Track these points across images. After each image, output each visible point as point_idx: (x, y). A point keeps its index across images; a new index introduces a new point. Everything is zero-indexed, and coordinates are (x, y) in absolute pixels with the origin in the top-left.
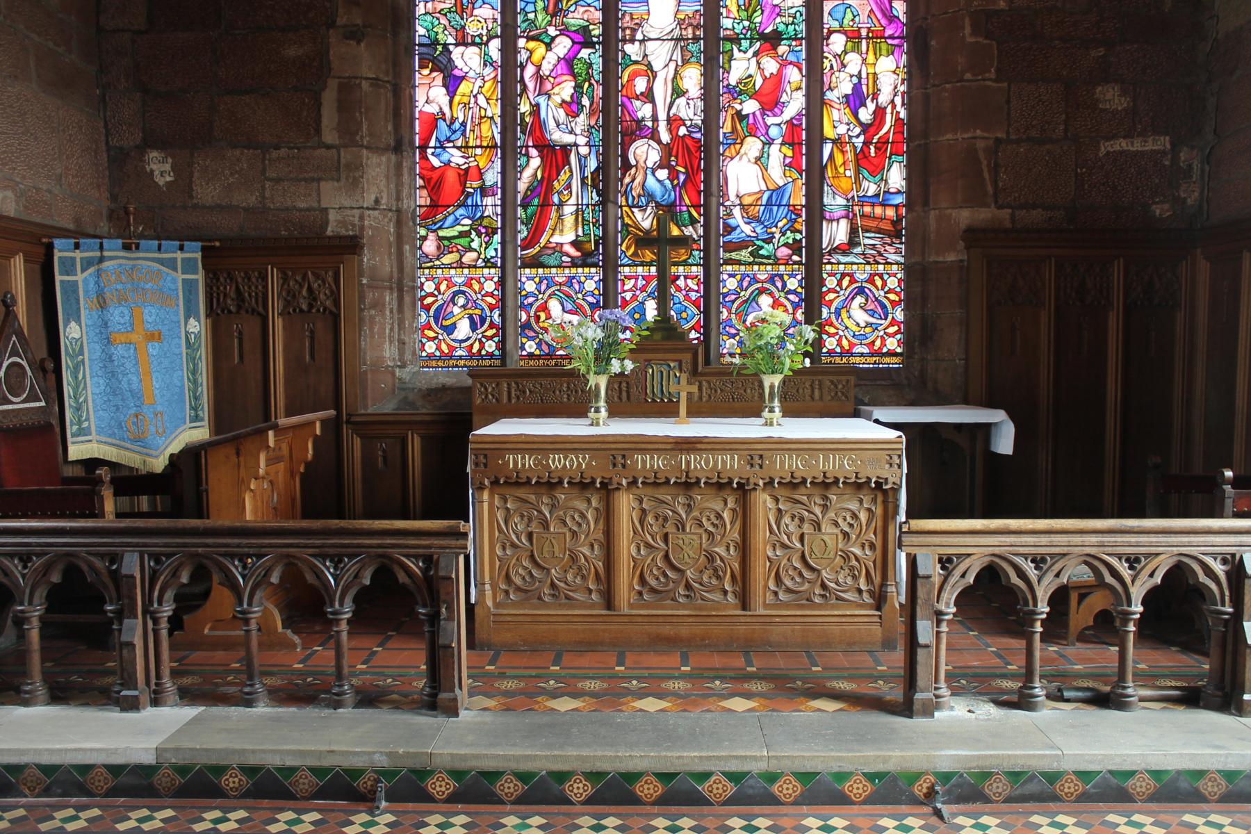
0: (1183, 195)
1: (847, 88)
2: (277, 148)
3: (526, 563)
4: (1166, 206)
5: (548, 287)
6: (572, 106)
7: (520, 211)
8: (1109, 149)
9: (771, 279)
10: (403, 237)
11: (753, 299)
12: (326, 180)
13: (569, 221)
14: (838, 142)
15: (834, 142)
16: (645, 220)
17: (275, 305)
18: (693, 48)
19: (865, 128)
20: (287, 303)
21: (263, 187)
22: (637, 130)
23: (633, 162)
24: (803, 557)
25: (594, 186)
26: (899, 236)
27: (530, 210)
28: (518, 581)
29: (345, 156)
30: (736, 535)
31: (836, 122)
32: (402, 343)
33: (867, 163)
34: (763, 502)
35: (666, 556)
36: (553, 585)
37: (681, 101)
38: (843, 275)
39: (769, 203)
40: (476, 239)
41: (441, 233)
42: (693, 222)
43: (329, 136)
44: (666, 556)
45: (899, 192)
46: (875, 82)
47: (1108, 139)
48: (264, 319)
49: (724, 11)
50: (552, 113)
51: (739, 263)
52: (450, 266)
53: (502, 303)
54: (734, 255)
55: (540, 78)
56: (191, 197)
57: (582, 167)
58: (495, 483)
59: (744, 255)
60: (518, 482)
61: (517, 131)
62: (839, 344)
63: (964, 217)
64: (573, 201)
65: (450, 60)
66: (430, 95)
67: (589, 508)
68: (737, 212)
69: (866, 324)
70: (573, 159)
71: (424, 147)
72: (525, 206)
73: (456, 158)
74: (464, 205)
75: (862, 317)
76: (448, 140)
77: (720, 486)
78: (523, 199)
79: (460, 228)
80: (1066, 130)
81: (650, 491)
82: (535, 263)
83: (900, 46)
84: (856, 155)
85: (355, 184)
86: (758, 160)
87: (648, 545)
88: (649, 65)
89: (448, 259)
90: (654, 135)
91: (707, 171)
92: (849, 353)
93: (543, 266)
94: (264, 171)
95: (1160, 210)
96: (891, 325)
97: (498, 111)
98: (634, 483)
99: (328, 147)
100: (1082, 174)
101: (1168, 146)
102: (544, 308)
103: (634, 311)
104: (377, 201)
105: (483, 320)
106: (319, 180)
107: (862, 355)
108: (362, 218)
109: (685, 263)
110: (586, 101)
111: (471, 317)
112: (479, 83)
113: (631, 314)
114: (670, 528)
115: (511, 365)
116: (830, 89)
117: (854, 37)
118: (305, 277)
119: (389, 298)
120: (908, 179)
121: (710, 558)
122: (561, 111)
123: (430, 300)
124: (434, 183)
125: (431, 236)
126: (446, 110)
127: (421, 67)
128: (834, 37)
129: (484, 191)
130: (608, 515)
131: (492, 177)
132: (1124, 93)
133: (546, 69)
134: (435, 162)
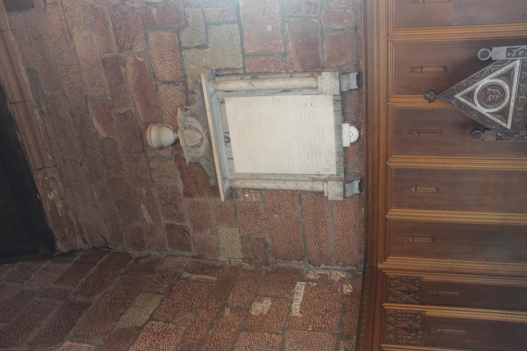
0: (339, 278)
4: (345, 286)
8: (297, 311)
47: (290, 310)
80: (278, 334)
95: (347, 289)
100: (313, 327)
101: (304, 283)
132: (260, 301)
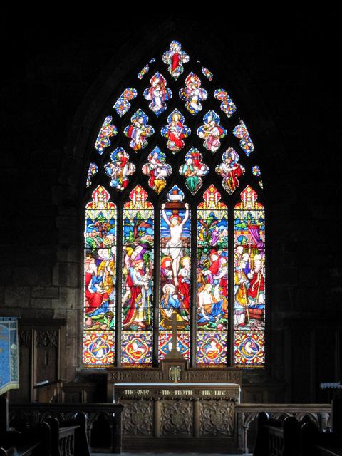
1: (244, 266)
2: (36, 286)
3: (130, 423)
5: (133, 338)
6: (143, 272)
7: (122, 310)
9: (215, 336)
10: (79, 319)
11: (209, 343)
12: (54, 298)
13: (141, 313)
14: (241, 286)
15: (239, 285)
16: (169, 313)
17: (34, 343)
18: (186, 250)
19: (250, 281)
20: (39, 343)
21: (31, 301)
22: (166, 280)
23: (165, 292)
24: (211, 421)
25: (151, 300)
26: (262, 320)
27: (127, 309)
28: (127, 428)
29: (61, 290)
30: (191, 415)
31: (239, 278)
32: (79, 358)
33: (251, 293)
34: (199, 404)
35: (171, 421)
36: (137, 429)
37: (182, 270)
38: (243, 334)
39: (214, 309)
40: (106, 320)
41: (93, 318)
42: (187, 314)
43: (56, 283)
44: (171, 421)
45: (263, 304)
46: (254, 265)
48: (30, 349)
49: (198, 238)
50: (136, 275)
51: (203, 330)
52: (96, 330)
53: (116, 342)
54: (202, 327)
55: (131, 261)
56: (4, 303)
57: (146, 294)
58: (121, 398)
59: (206, 327)
60: (129, 398)
61: (120, 281)
62: (241, 360)
63: (283, 315)
64: (142, 306)
65: (97, 254)
66: (90, 267)
67: (149, 407)
68: (203, 311)
69: (251, 351)
70: (143, 290)
71: (87, 286)
72: (124, 308)
73: (99, 290)
74: (102, 307)
75: (249, 350)
76: (96, 283)
77: (187, 399)
78: (125, 305)
79: (100, 316)
81: (166, 401)
82: (128, 329)
83: (263, 251)
84: (247, 290)
85: (65, 300)
86: (210, 292)
87: (165, 418)
88: (171, 257)
89: (94, 328)
90: (172, 282)
91: (192, 295)
92: (245, 363)
93: (131, 330)
94: (31, 294)
96: (260, 353)
97: (115, 273)
98: (161, 399)
99: (55, 287)
102: (131, 346)
103: (164, 347)
104: (72, 306)
105: (108, 349)
106: (51, 298)
107: (250, 364)
108: (67, 312)
109: (184, 330)
110: (147, 269)
111: (103, 349)
112: (108, 262)
113: (163, 349)
114: (172, 412)
115: (118, 366)
116: (238, 266)
117: (246, 247)
118: (46, 333)
119: (75, 341)
120: (266, 300)
121: (184, 422)
122: (138, 274)
123: (88, 342)
124: (91, 299)
125: (89, 318)
126: (96, 272)
127: (87, 256)
128: (239, 248)
129: (109, 302)
130: (154, 408)
131: (113, 297)
133: (133, 257)
134: (91, 291)
